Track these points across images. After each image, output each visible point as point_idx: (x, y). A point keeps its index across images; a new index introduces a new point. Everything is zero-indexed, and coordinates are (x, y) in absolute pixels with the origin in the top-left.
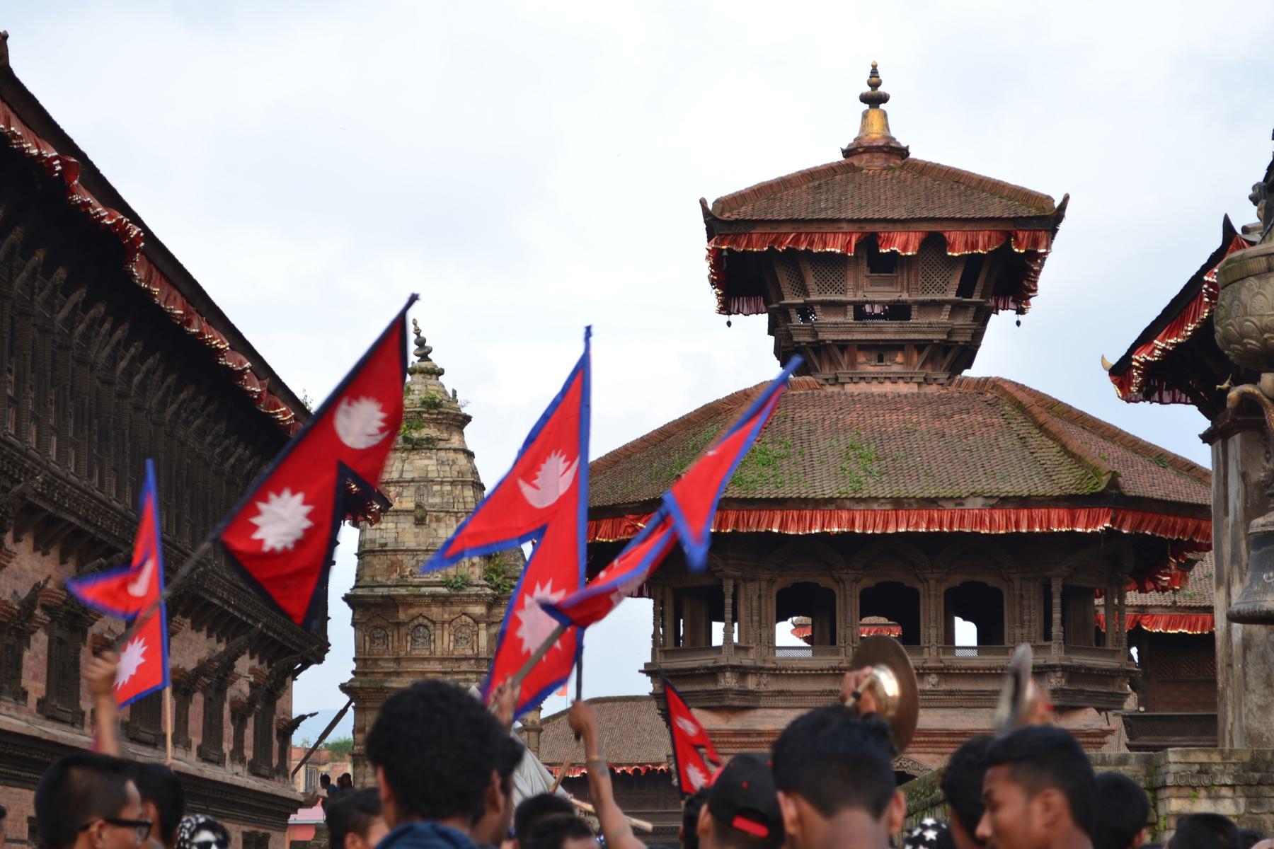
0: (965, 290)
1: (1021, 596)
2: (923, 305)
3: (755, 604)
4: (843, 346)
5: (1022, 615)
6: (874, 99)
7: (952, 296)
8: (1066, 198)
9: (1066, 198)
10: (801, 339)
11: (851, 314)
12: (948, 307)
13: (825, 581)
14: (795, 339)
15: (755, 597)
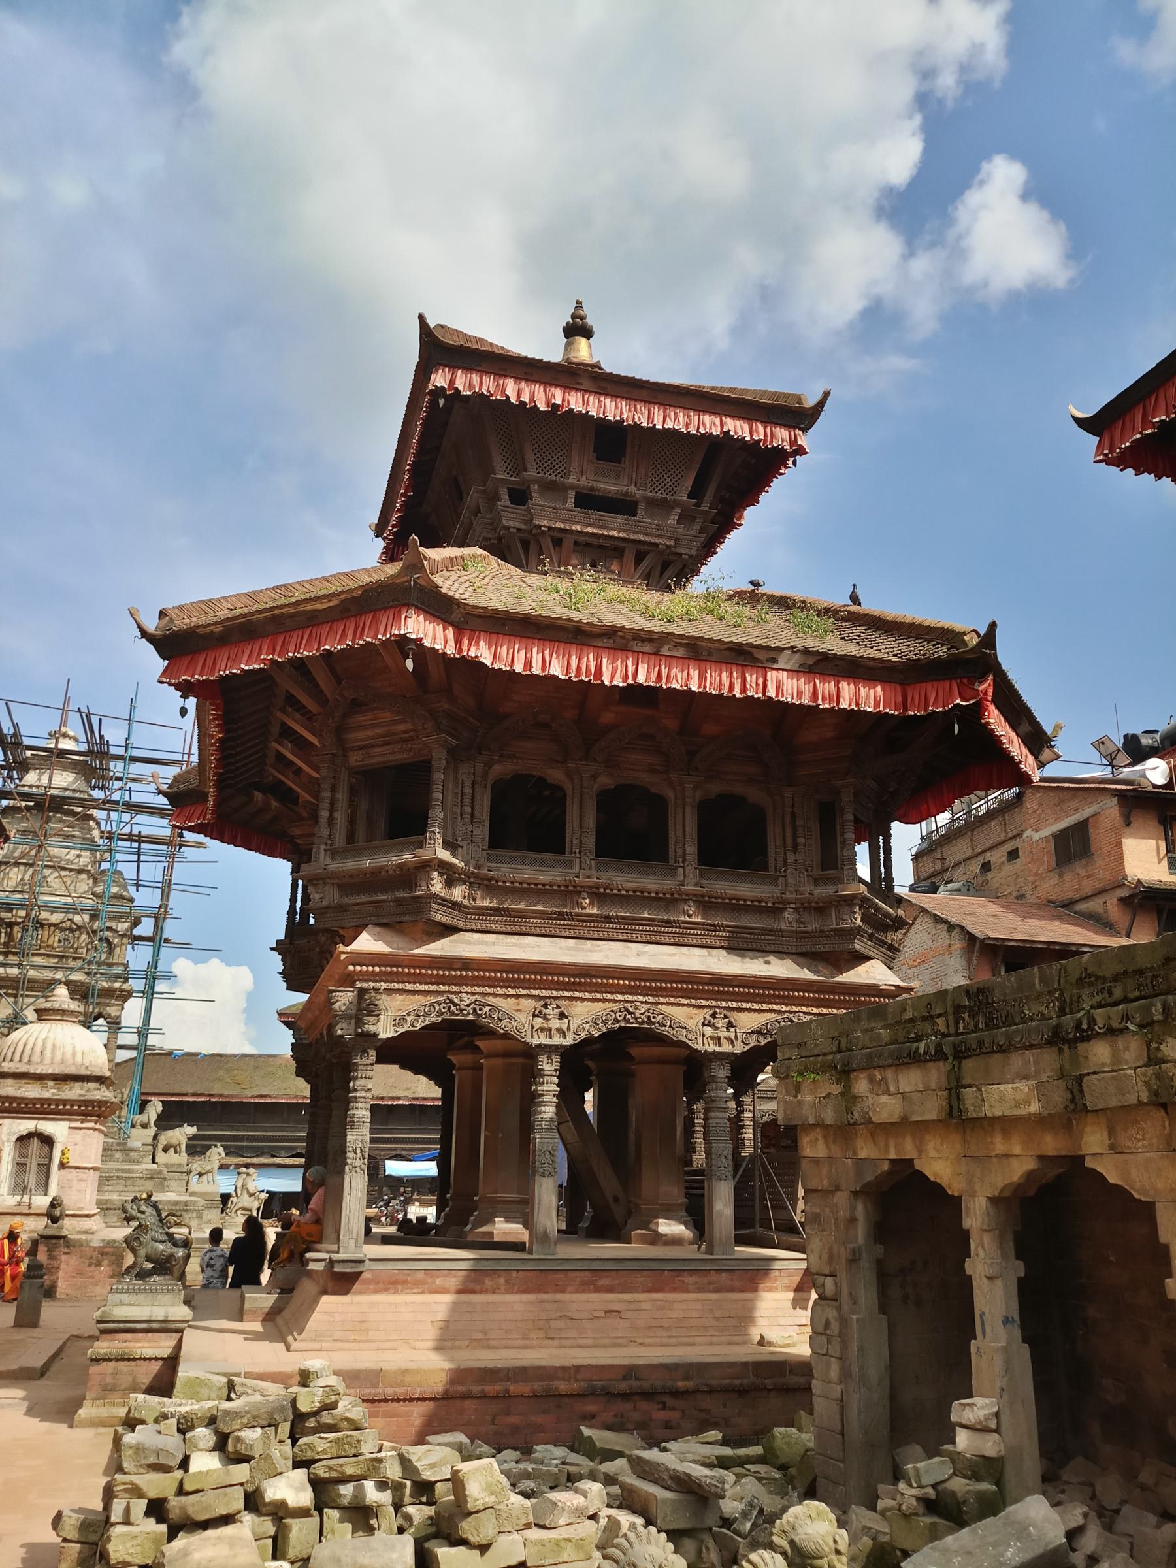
0: (696, 492)
1: (793, 814)
2: (652, 503)
3: (468, 790)
4: (558, 539)
5: (795, 838)
6: (577, 329)
7: (683, 497)
8: (826, 394)
9: (826, 394)
10: (511, 523)
11: (571, 501)
12: (678, 510)
13: (555, 775)
14: (505, 523)
15: (468, 783)
